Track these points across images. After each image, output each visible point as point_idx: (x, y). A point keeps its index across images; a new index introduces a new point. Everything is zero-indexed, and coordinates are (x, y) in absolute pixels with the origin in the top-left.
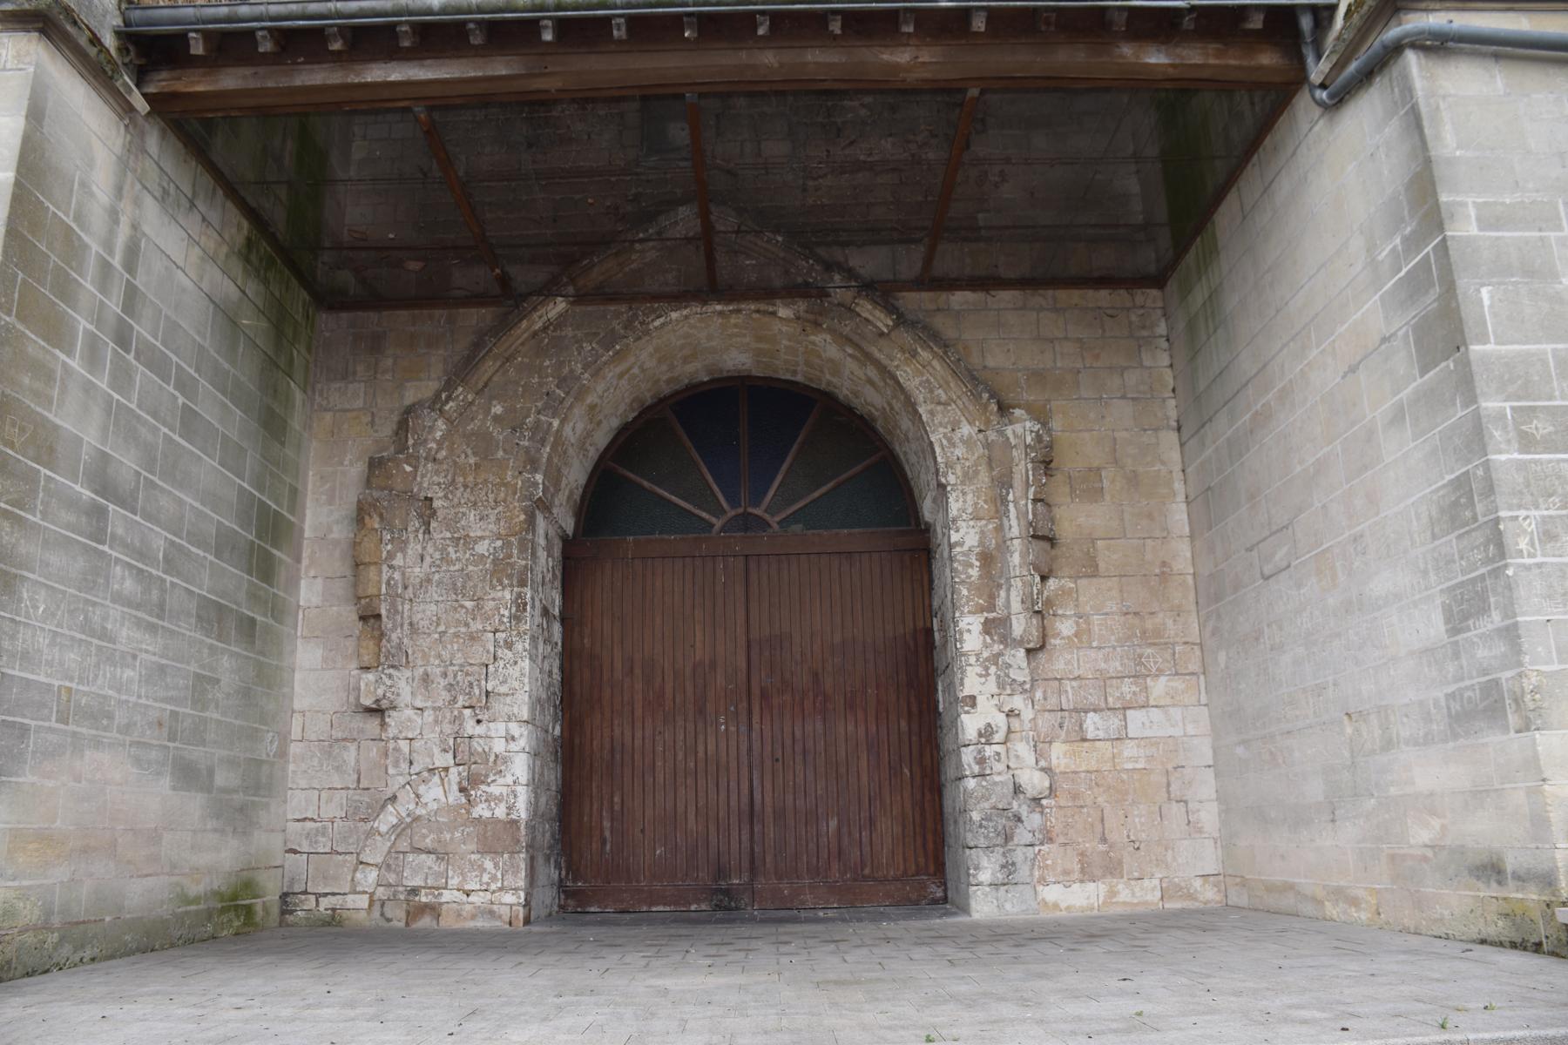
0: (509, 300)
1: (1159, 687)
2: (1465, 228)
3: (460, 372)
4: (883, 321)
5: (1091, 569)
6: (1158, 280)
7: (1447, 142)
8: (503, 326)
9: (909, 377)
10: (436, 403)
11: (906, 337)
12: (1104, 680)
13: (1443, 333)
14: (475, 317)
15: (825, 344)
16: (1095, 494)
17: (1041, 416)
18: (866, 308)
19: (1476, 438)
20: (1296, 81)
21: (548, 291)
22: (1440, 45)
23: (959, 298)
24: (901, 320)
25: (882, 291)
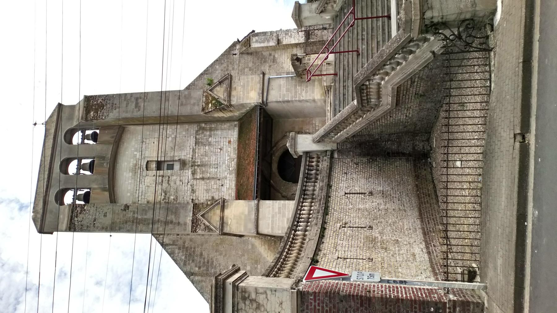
0: (270, 186)
1: (314, 122)
2: (281, 100)
3: (279, 192)
4: (275, 148)
5: (302, 128)
6: (272, 120)
7: (274, 100)
8: (273, 187)
9: (281, 146)
10: (281, 194)
11: (277, 146)
12: (313, 127)
13: (288, 102)
14: (272, 189)
15: (277, 155)
16: (294, 127)
17: (286, 132)
18: (274, 149)
19: (296, 101)
20: (263, 108)
21: (270, 182)
22: (267, 99)
23: (273, 140)
24: (275, 146)
25: (272, 148)
